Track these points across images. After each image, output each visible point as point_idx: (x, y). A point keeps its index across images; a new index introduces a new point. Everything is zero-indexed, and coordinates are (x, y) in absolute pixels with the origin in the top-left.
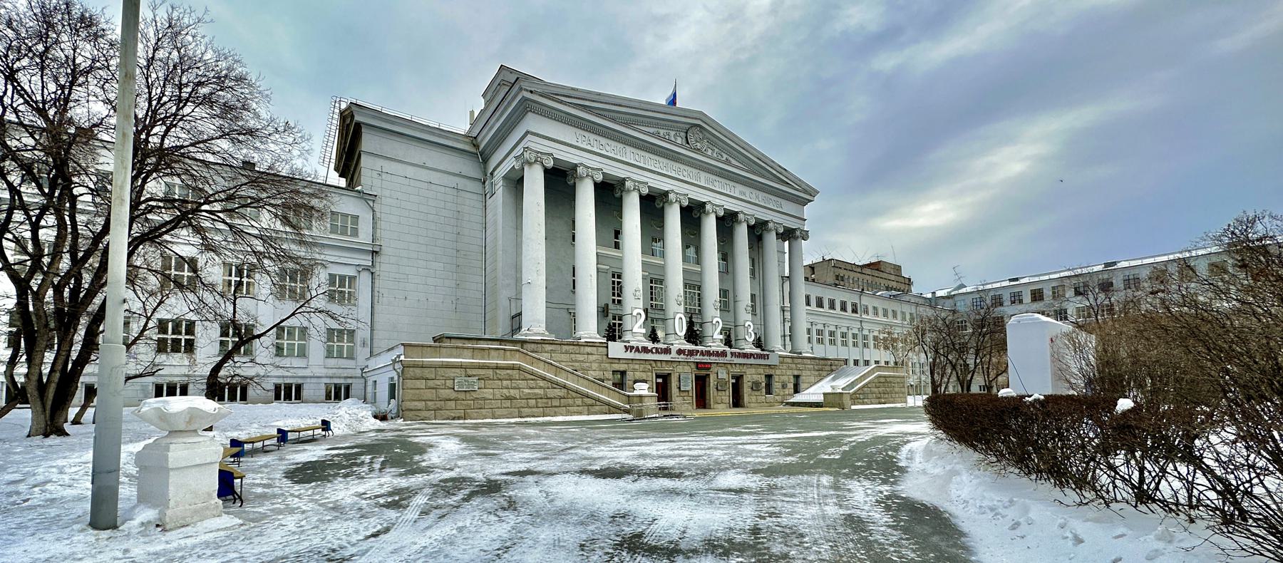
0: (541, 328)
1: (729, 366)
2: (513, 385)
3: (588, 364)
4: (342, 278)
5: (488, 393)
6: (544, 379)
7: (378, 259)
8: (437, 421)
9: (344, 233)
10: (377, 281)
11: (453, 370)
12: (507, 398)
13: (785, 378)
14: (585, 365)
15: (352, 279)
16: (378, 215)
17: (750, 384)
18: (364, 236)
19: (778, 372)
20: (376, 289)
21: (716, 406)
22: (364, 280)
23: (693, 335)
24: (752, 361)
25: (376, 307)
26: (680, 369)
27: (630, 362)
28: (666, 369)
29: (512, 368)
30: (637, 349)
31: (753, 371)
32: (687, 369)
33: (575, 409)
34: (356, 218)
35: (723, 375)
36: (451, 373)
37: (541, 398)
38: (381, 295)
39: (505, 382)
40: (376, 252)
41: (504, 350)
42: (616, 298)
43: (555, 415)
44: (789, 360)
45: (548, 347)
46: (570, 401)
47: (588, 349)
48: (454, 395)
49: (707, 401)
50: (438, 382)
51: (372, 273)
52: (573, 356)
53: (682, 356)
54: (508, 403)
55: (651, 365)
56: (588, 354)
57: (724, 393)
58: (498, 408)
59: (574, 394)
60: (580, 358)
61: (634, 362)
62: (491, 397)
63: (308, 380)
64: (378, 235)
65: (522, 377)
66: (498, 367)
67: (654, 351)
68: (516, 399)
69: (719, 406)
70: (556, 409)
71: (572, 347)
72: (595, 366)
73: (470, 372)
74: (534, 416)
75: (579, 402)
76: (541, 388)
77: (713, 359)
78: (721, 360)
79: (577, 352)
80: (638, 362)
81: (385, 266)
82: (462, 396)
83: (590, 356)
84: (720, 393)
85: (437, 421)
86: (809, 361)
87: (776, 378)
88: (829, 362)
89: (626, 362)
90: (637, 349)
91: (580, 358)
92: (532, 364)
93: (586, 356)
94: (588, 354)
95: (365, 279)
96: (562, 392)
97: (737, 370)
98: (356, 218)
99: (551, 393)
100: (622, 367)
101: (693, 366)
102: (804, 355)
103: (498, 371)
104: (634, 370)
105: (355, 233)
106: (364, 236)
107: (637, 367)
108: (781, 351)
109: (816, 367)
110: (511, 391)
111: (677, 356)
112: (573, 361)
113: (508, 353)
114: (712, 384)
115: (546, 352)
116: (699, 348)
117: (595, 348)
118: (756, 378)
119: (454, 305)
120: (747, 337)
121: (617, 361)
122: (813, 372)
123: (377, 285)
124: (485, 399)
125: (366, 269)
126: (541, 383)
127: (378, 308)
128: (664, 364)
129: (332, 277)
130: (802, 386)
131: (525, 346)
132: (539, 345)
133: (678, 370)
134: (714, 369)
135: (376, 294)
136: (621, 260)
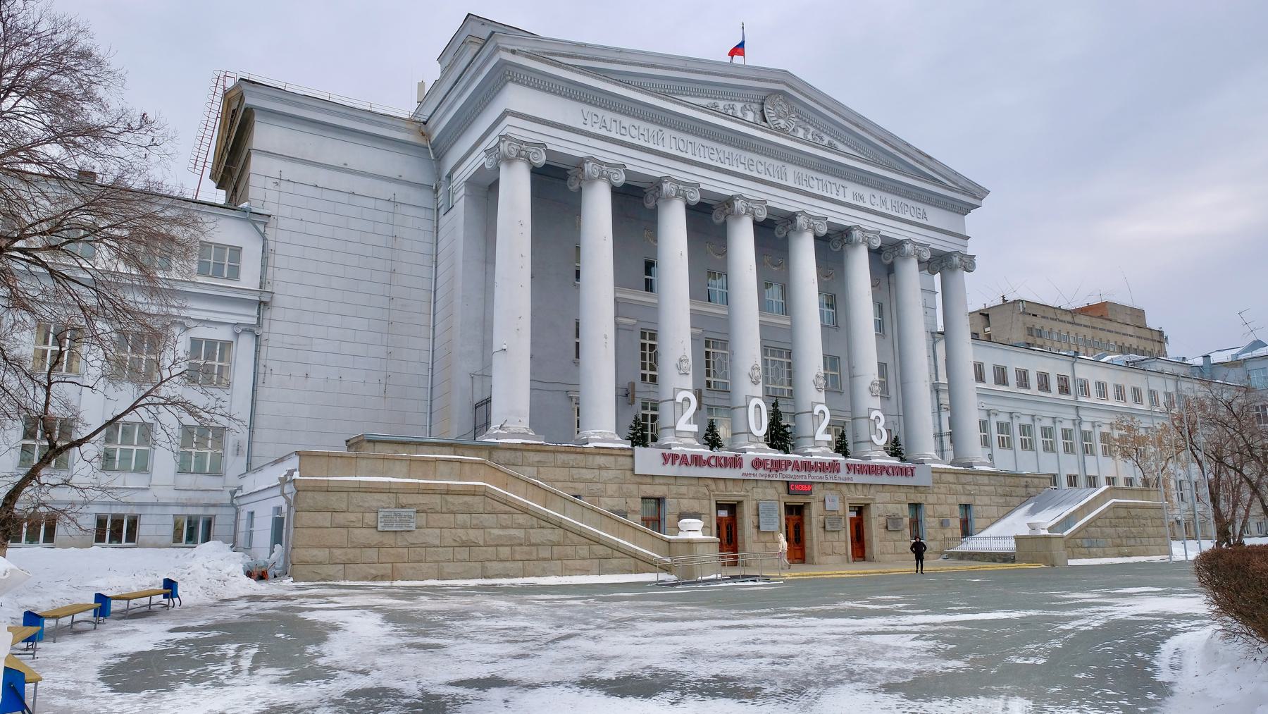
0: (521, 422)
1: (844, 489)
2: (475, 522)
3: (599, 486)
4: (211, 344)
5: (432, 536)
6: (525, 511)
7: (267, 314)
8: (348, 583)
9: (218, 274)
10: (263, 350)
11: (377, 496)
12: (464, 544)
13: (944, 510)
14: (595, 487)
15: (226, 345)
16: (271, 245)
17: (882, 520)
18: (249, 279)
19: (931, 499)
20: (262, 362)
21: (823, 558)
23: (779, 436)
24: (884, 479)
25: (260, 390)
26: (758, 493)
27: (672, 481)
28: (733, 494)
29: (473, 492)
31: (886, 496)
32: (771, 493)
33: (578, 563)
34: (237, 251)
36: (372, 500)
37: (521, 545)
38: (268, 371)
39: (460, 517)
40: (265, 303)
41: (460, 461)
42: (648, 372)
43: (544, 574)
44: (951, 478)
46: (569, 550)
47: (601, 460)
48: (375, 538)
49: (807, 551)
50: (352, 517)
51: (257, 336)
52: (574, 471)
53: (761, 471)
54: (463, 553)
55: (707, 486)
56: (600, 468)
57: (836, 535)
58: (449, 561)
59: (576, 539)
60: (587, 474)
61: (679, 481)
62: (437, 542)
63: (149, 510)
64: (269, 276)
65: (489, 509)
66: (448, 491)
67: (713, 462)
68: (478, 545)
69: (830, 559)
70: (545, 564)
71: (572, 456)
72: (612, 488)
73: (404, 499)
74: (508, 576)
75: (584, 551)
76: (520, 527)
78: (829, 477)
79: (582, 464)
80: (686, 482)
81: (278, 326)
82: (388, 540)
83: (604, 473)
84: (829, 536)
85: (348, 583)
86: (985, 480)
87: (928, 510)
89: (666, 481)
91: (587, 474)
92: (505, 487)
93: (597, 472)
94: (600, 468)
95: (245, 346)
96: (555, 535)
97: (858, 497)
98: (237, 251)
99: (537, 535)
100: (658, 491)
102: (977, 468)
103: (449, 498)
104: (680, 496)
105: (235, 274)
106: (249, 279)
107: (683, 490)
108: (935, 461)
109: (1000, 490)
110: (471, 532)
111: (753, 471)
113: (467, 467)
114: (814, 521)
115: (529, 465)
116: (792, 456)
117: (612, 459)
118: (893, 509)
119: (383, 387)
120: (874, 438)
121: (649, 480)
123: (263, 355)
124: (426, 546)
125: (248, 329)
126: (521, 519)
127: (263, 392)
128: (730, 484)
129: (195, 343)
130: (976, 523)
131: (496, 454)
132: (519, 454)
133: (756, 496)
134: (818, 493)
135: (261, 369)
136: (655, 309)
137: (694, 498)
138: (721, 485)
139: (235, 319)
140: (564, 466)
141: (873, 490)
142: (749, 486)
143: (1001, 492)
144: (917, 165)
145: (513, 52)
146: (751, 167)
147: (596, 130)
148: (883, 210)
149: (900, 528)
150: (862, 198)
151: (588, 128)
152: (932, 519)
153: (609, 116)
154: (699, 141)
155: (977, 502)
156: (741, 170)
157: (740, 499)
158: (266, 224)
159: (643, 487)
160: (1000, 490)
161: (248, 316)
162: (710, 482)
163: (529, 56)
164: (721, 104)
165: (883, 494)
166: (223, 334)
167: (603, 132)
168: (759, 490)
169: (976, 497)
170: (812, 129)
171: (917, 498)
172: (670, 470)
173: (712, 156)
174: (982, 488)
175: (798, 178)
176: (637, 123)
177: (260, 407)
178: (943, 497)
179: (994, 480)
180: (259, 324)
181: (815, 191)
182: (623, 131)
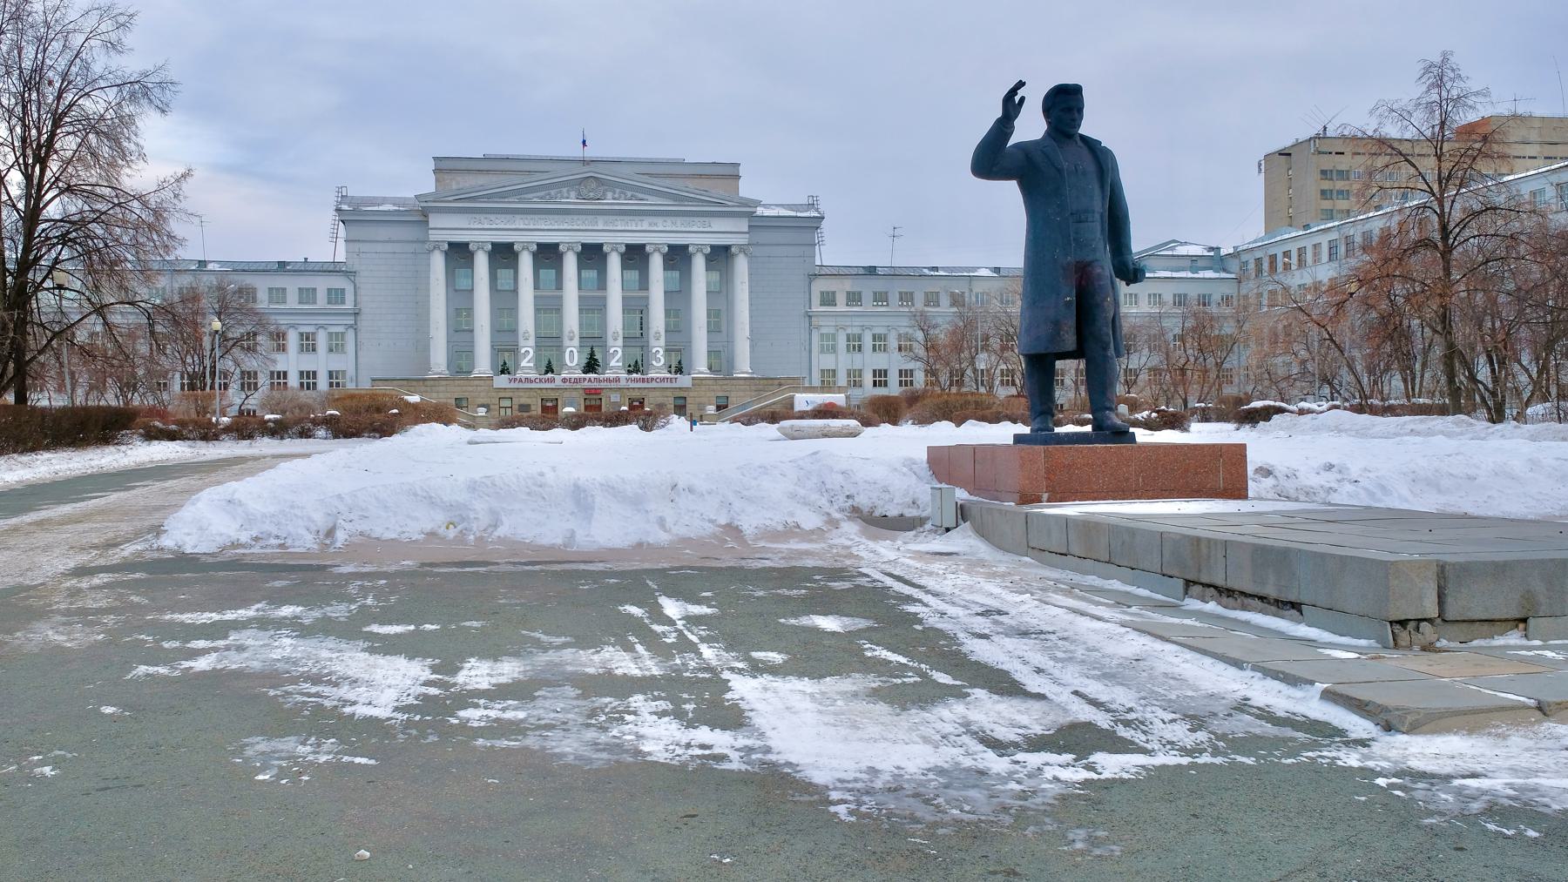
4: (337, 334)
9: (336, 303)
15: (343, 334)
18: (349, 305)
19: (691, 394)
22: (350, 335)
23: (591, 366)
25: (359, 354)
26: (566, 394)
28: (553, 395)
31: (658, 393)
32: (575, 394)
35: (615, 398)
44: (710, 382)
45: (444, 383)
60: (471, 389)
64: (358, 300)
77: (603, 385)
81: (364, 323)
86: (742, 382)
88: (776, 382)
90: (521, 380)
91: (471, 389)
95: (350, 335)
97: (636, 394)
101: (582, 392)
105: (343, 302)
107: (522, 394)
109: (753, 388)
118: (660, 400)
122: (749, 393)
125: (351, 326)
127: (359, 353)
131: (426, 383)
134: (603, 396)
139: (345, 322)
142: (560, 391)
144: (698, 197)
148: (674, 229)
150: (656, 224)
151: (472, 226)
153: (482, 216)
154: (536, 217)
163: (435, 201)
164: (553, 192)
166: (340, 329)
170: (618, 190)
171: (682, 394)
172: (513, 385)
175: (606, 223)
176: (499, 216)
177: (360, 360)
179: (748, 382)
180: (356, 324)
181: (619, 228)
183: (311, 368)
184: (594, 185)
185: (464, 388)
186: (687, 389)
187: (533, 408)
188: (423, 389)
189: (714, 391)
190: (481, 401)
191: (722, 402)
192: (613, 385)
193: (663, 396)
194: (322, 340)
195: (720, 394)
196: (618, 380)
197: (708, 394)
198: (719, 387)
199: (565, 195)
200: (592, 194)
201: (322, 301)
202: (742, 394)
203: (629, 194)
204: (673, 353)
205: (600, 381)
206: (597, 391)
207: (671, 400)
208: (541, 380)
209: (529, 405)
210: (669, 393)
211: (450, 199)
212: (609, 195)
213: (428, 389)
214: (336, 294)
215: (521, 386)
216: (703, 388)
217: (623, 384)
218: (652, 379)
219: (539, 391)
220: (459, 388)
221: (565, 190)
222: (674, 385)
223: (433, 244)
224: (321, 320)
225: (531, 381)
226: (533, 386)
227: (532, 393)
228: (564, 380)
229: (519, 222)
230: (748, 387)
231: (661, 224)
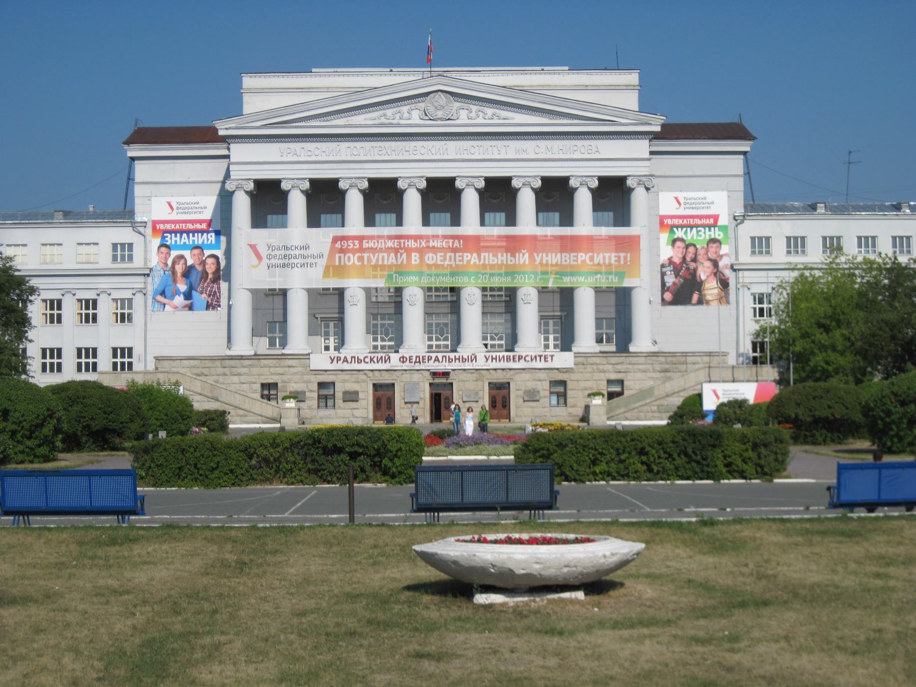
1: (484, 372)
3: (289, 377)
14: (285, 378)
15: (130, 301)
18: (138, 262)
19: (573, 376)
26: (406, 377)
28: (386, 379)
30: (346, 360)
31: (526, 376)
32: (416, 377)
34: (131, 245)
55: (366, 374)
56: (289, 367)
67: (368, 360)
79: (278, 365)
83: (292, 369)
86: (642, 360)
93: (287, 369)
94: (289, 367)
97: (499, 378)
98: (131, 245)
101: (427, 374)
104: (344, 381)
105: (131, 258)
107: (347, 377)
111: (401, 364)
112: (272, 374)
115: (244, 367)
118: (531, 385)
125: (140, 291)
137: (355, 382)
138: (376, 373)
140: (265, 366)
141: (512, 372)
143: (658, 369)
145: (227, 129)
146: (415, 152)
147: (290, 159)
148: (549, 156)
149: (537, 398)
151: (285, 159)
152: (573, 392)
155: (629, 378)
156: (406, 157)
157: (393, 382)
158: (145, 227)
159: (318, 376)
160: (658, 368)
161: (138, 282)
162: (367, 372)
164: (389, 112)
165: (523, 375)
166: (127, 295)
167: (296, 159)
168: (408, 376)
169: (628, 374)
170: (474, 108)
173: (380, 153)
174: (636, 367)
178: (589, 375)
182: (310, 153)
183: (90, 344)
184: (442, 99)
185: (272, 370)
186: (567, 370)
187: (361, 395)
188: (220, 370)
189: (604, 372)
190: (293, 387)
191: (617, 389)
192: (468, 365)
193: (535, 380)
194: (105, 310)
195: (613, 376)
196: (474, 358)
197: (597, 376)
198: (610, 367)
199: (406, 115)
200: (440, 114)
201: (104, 260)
202: (640, 375)
203: (490, 111)
204: (551, 322)
205: (450, 360)
206: (446, 374)
207: (546, 385)
208: (372, 360)
209: (357, 393)
210: (542, 375)
211: (258, 124)
212: (463, 114)
213: (227, 371)
214: (123, 250)
215: (346, 366)
216: (589, 368)
217: (481, 363)
218: (520, 358)
219: (370, 374)
220: (266, 370)
221: (405, 109)
222: (549, 365)
223: (235, 183)
224: (103, 283)
225: (359, 361)
226: (362, 366)
227: (362, 377)
228: (403, 360)
229: (344, 150)
230: (649, 367)
231: (530, 147)
